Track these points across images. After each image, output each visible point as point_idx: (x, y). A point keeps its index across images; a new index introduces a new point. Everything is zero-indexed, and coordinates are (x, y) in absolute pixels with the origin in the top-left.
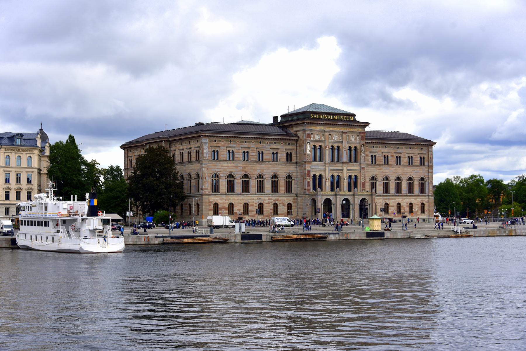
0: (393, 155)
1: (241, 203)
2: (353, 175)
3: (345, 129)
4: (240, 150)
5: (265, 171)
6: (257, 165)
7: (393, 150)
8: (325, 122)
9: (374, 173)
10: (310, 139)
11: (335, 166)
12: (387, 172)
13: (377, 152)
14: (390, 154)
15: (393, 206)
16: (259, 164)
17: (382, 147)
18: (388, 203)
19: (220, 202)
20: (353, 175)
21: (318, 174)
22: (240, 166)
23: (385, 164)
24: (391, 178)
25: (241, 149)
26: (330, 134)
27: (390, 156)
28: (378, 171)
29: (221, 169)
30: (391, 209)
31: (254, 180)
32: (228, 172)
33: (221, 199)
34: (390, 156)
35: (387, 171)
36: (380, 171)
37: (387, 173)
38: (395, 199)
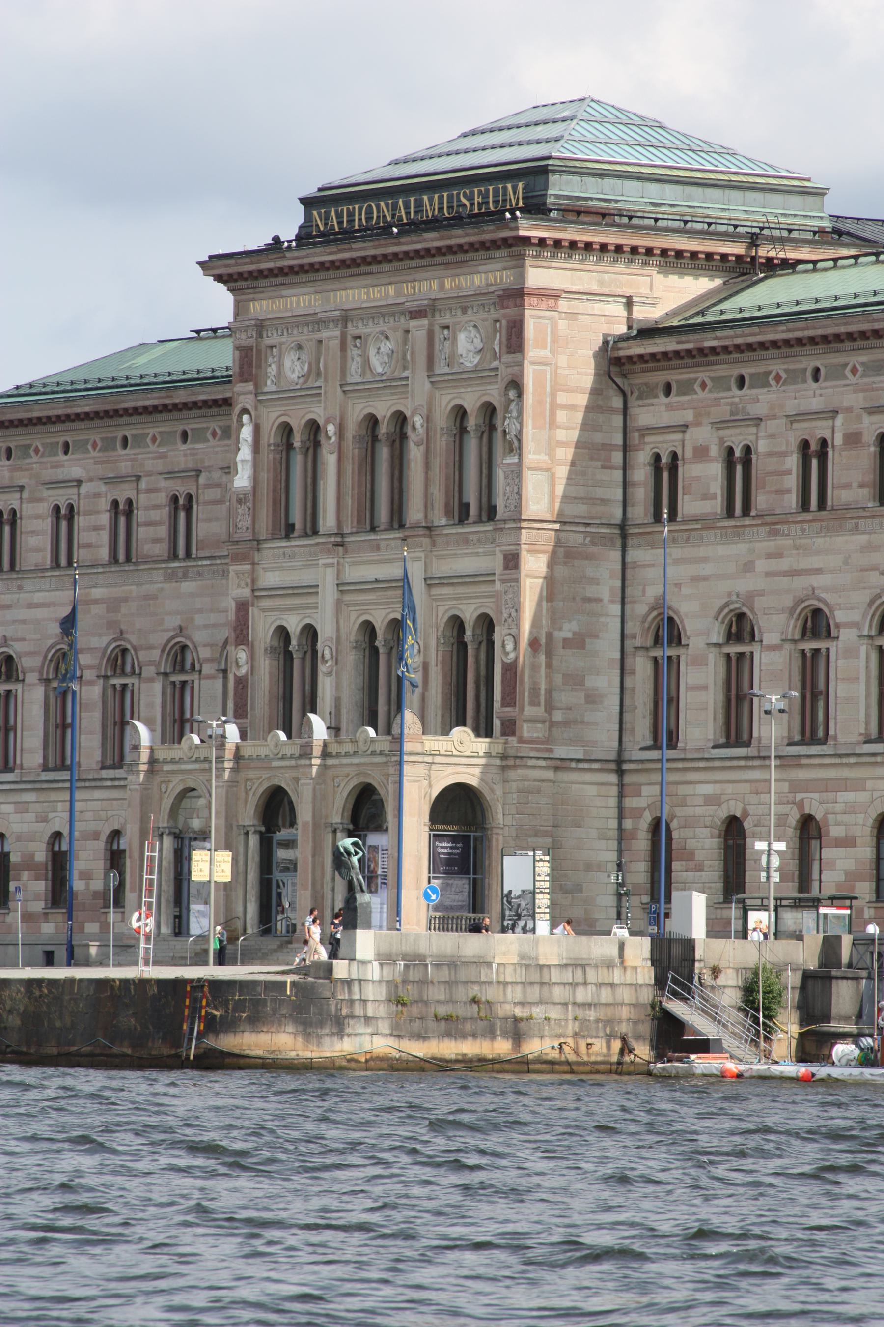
0: (854, 427)
1: (96, 836)
2: (469, 614)
3: (425, 285)
4: (97, 495)
5: (199, 620)
6: (166, 586)
7: (857, 389)
8: (627, 240)
9: (744, 585)
10: (250, 386)
11: (375, 556)
12: (818, 571)
13: (758, 421)
14: (839, 421)
15: (848, 842)
16: (171, 577)
17: (795, 377)
18: (818, 816)
19: (17, 828)
20: (469, 614)
21: (294, 624)
22: (96, 602)
23: (805, 505)
24: (840, 616)
25: (103, 488)
26: (357, 332)
27: (839, 440)
28: (761, 565)
29: (24, 622)
30: (832, 865)
31: (151, 680)
32: (50, 642)
33: (22, 808)
34: (839, 440)
35: (815, 562)
36: (775, 565)
37: (816, 581)
38: (858, 785)
